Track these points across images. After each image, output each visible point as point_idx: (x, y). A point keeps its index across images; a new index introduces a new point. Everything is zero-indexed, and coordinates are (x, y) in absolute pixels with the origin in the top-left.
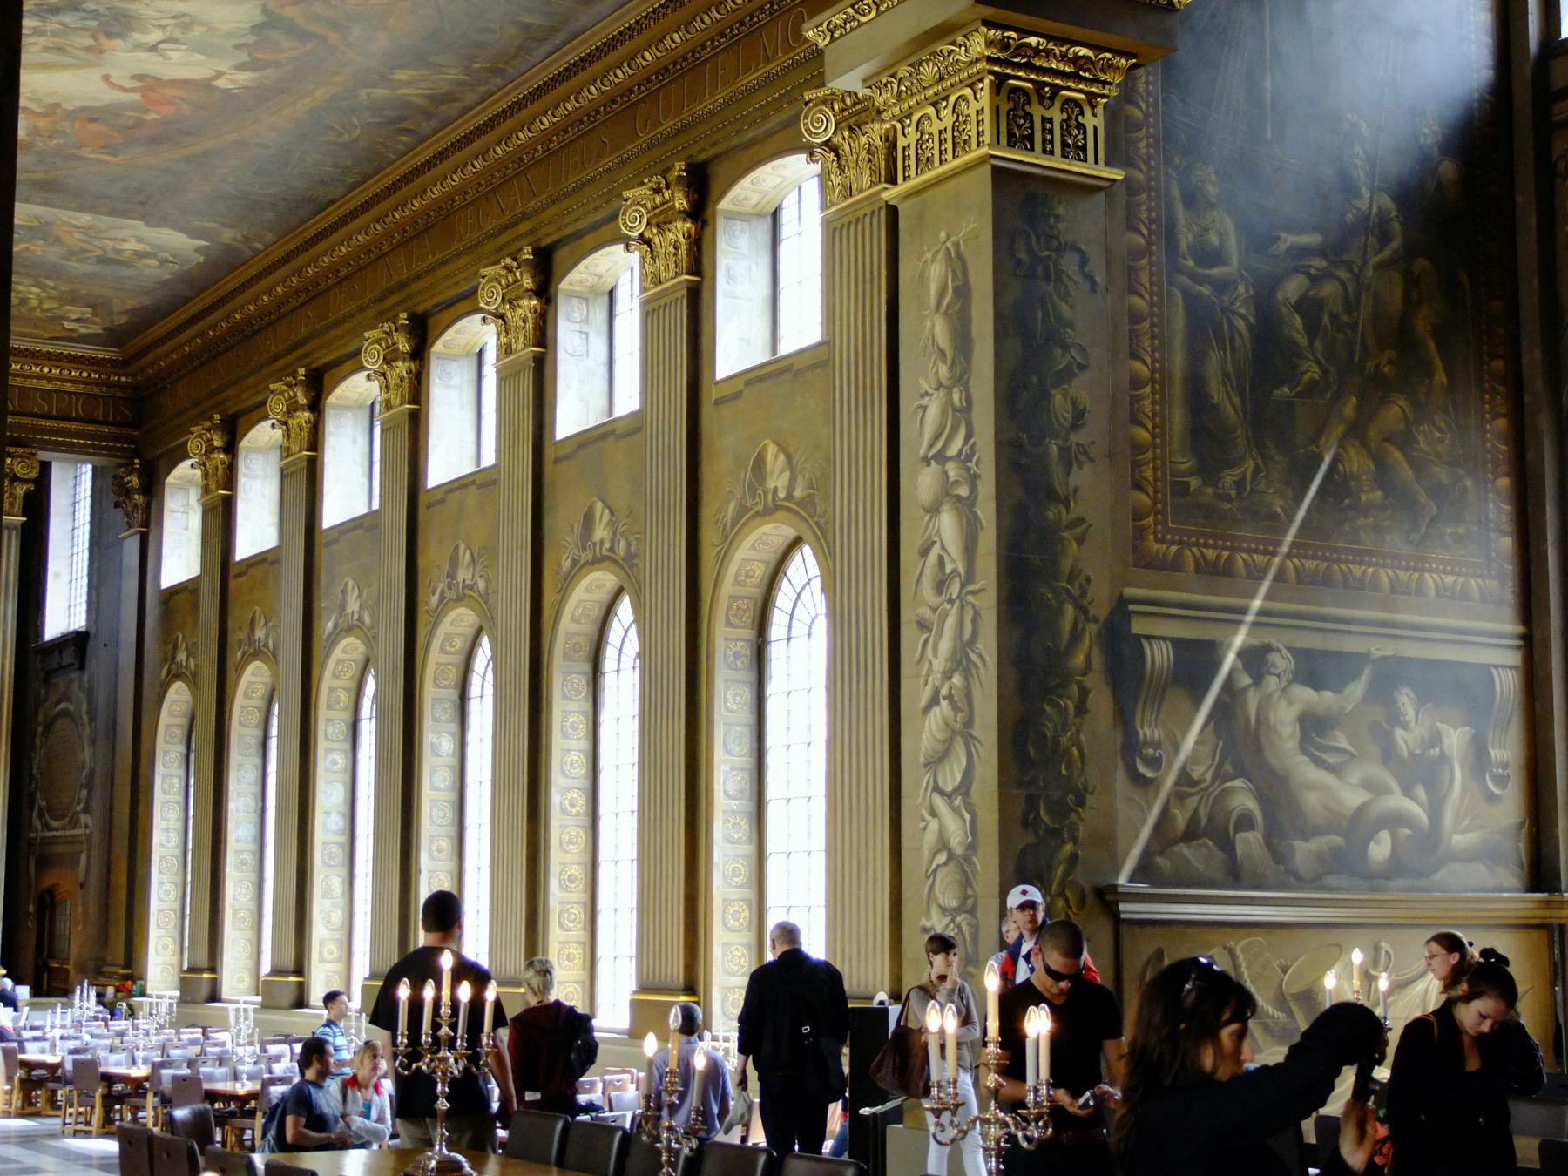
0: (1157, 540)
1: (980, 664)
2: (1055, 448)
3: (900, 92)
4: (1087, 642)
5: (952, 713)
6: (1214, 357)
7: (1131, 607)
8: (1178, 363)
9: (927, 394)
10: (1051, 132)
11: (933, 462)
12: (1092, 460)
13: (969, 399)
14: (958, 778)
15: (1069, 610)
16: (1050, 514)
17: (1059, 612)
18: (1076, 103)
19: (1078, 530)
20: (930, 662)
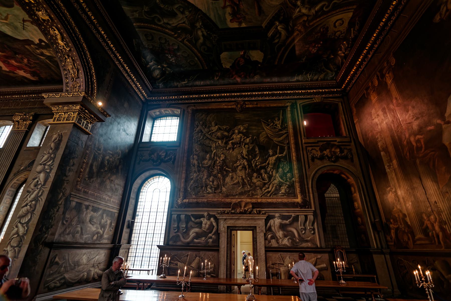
0: (79, 186)
1: (41, 200)
2: (68, 169)
3: (58, 109)
4: (62, 200)
5: (30, 208)
6: (95, 163)
7: (72, 195)
8: (90, 161)
9: (45, 154)
10: (84, 124)
11: (42, 165)
12: (73, 172)
13: (55, 156)
14: (27, 220)
15: (61, 194)
16: (64, 178)
17: (60, 194)
18: (89, 122)
19: (67, 182)
20: (28, 199)
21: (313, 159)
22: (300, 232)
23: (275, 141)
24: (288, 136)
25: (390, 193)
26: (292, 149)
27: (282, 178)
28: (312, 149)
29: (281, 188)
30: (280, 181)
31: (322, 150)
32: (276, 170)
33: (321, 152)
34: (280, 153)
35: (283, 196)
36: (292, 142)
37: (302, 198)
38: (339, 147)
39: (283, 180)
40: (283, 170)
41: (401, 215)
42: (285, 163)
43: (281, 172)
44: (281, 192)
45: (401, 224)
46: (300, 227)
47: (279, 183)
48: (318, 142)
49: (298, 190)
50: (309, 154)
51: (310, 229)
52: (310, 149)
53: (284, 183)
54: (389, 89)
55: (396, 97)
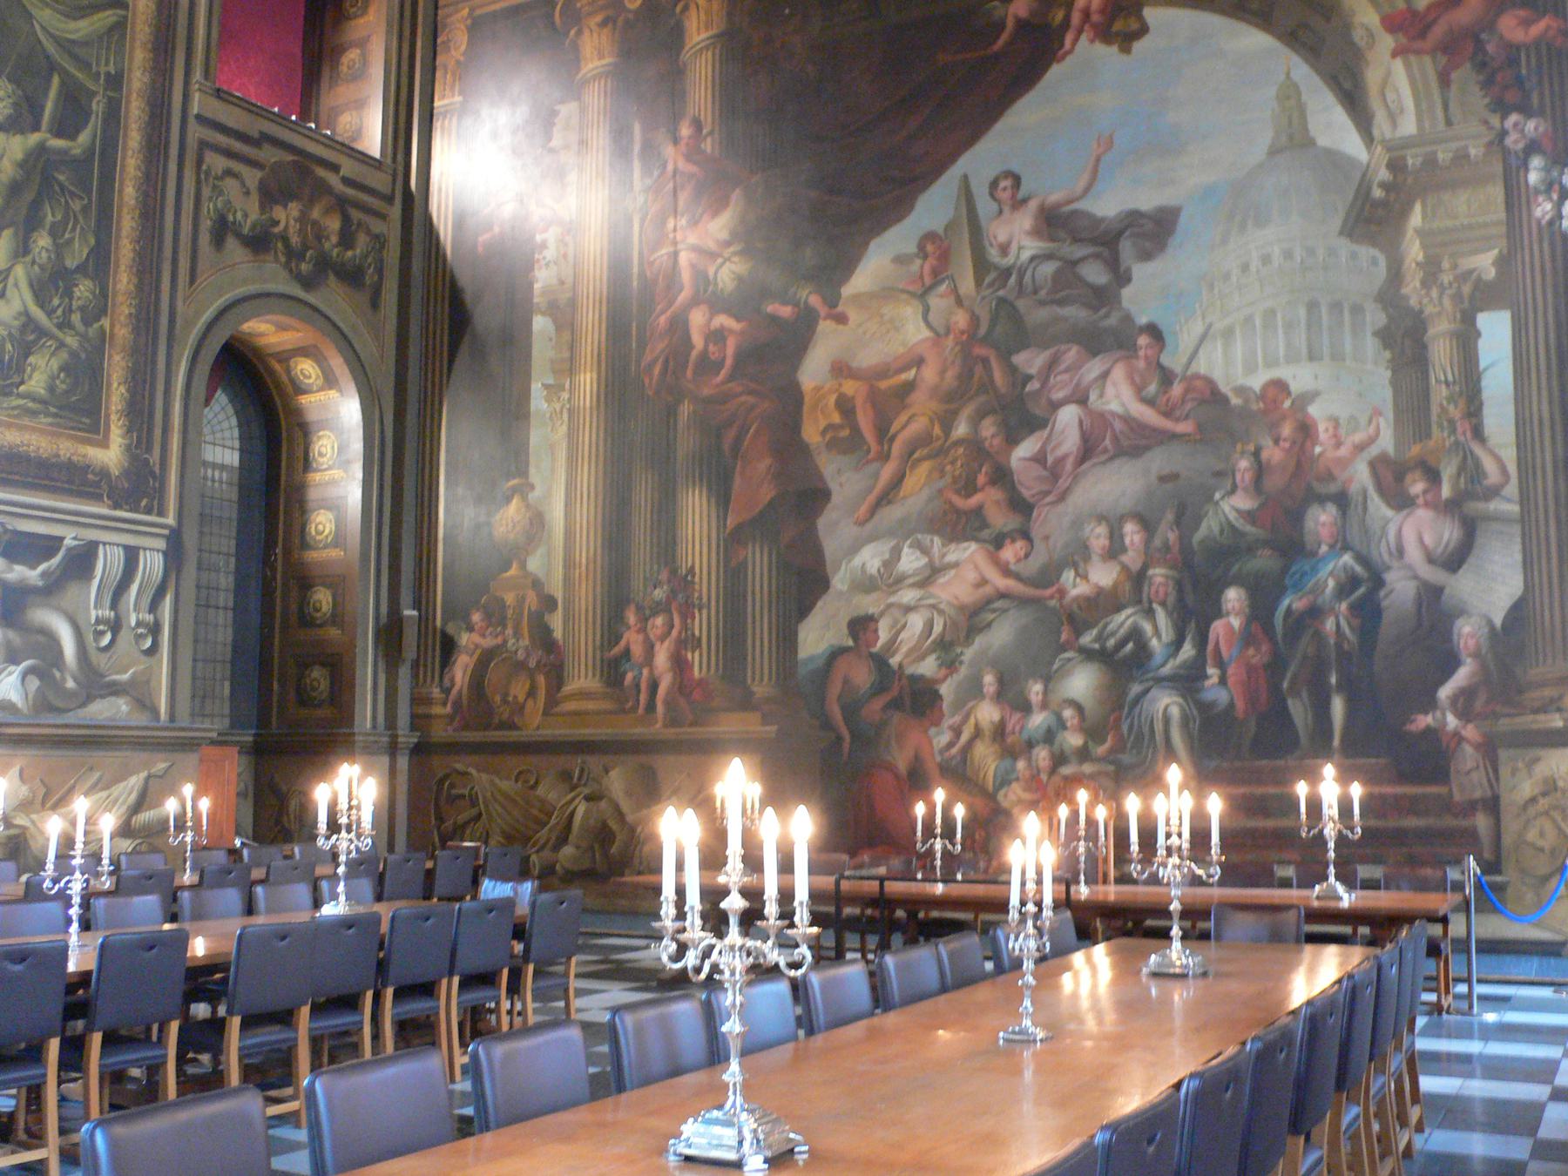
21: (222, 229)
22: (90, 637)
23: (43, 28)
24: (120, 27)
25: (515, 502)
26: (126, 128)
27: (41, 301)
28: (229, 173)
29: (31, 359)
30: (26, 313)
31: (270, 195)
32: (16, 234)
33: (262, 207)
34: (59, 134)
35: (33, 413)
36: (138, 79)
37: (128, 448)
38: (342, 205)
39: (50, 314)
40: (59, 249)
41: (532, 600)
42: (76, 205)
43: (44, 255)
44: (22, 388)
45: (517, 634)
46: (93, 614)
47: (24, 326)
48: (266, 139)
49: (116, 396)
50: (206, 192)
51: (139, 624)
52: (217, 162)
53: (52, 337)
54: (685, 64)
55: (702, 117)
